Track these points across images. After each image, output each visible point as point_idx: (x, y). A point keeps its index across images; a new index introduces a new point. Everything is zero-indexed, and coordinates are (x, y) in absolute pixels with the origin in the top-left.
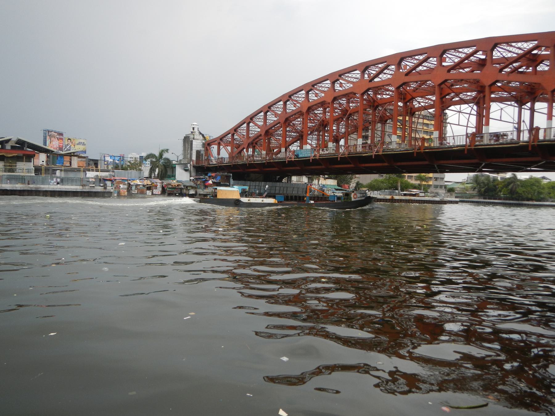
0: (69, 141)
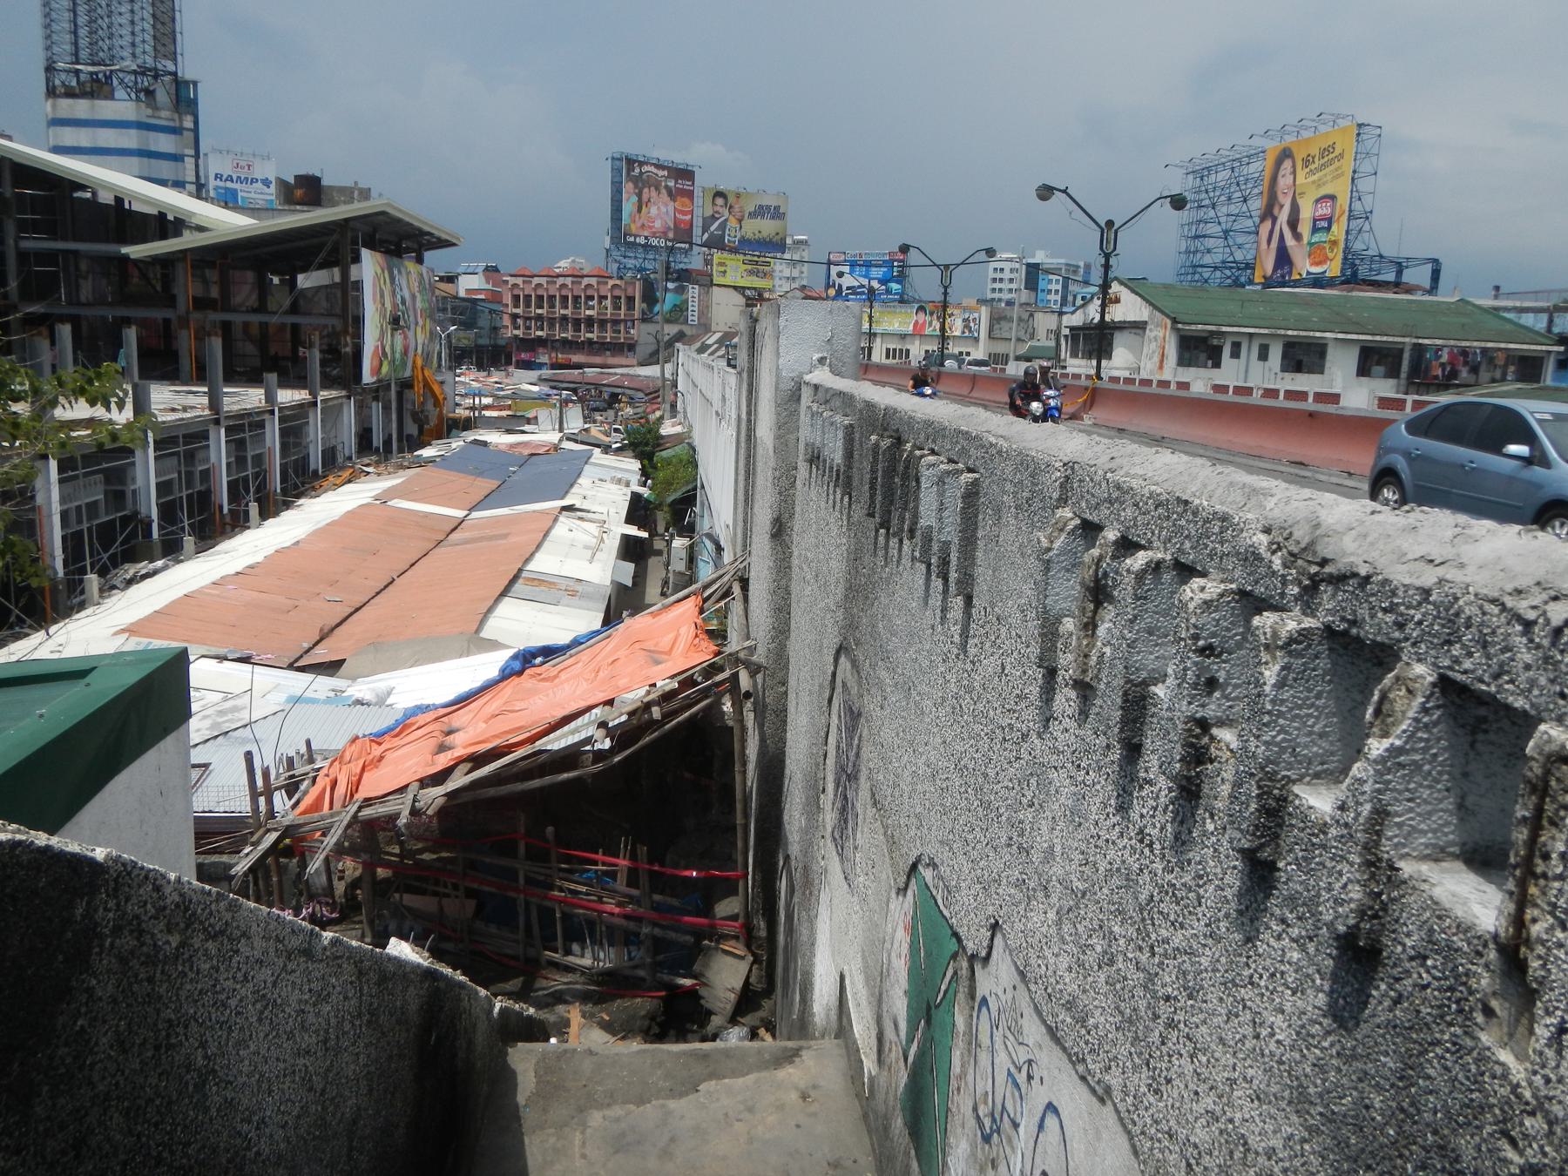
0: (720, 201)
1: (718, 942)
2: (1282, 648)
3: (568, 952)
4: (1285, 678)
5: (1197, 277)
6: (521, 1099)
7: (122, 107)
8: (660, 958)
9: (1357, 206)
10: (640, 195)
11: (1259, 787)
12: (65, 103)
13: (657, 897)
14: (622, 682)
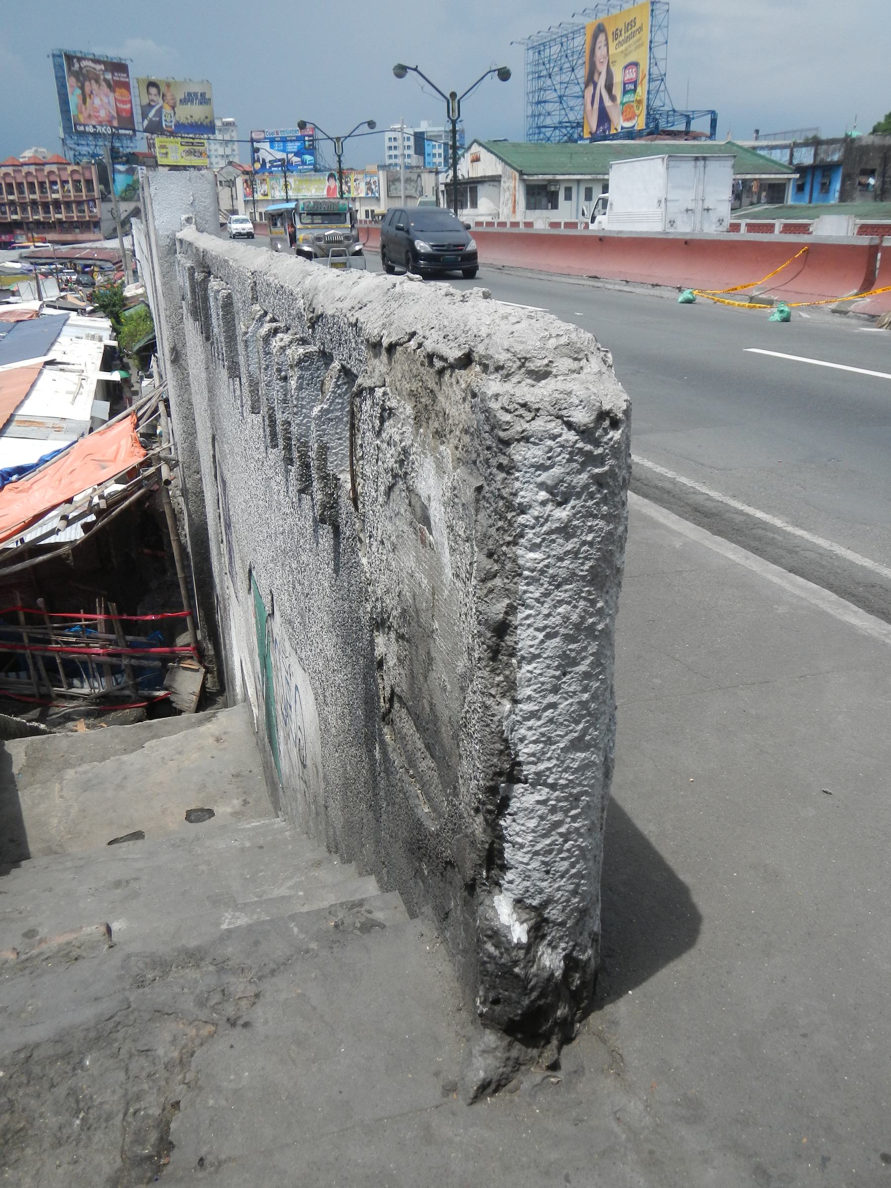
0: (153, 90)
1: (179, 662)
2: (296, 365)
3: (71, 686)
4: (301, 384)
5: (542, 136)
6: (15, 770)
8: (139, 680)
9: (655, 70)
10: (82, 88)
11: (299, 452)
13: (129, 638)
14: (77, 485)
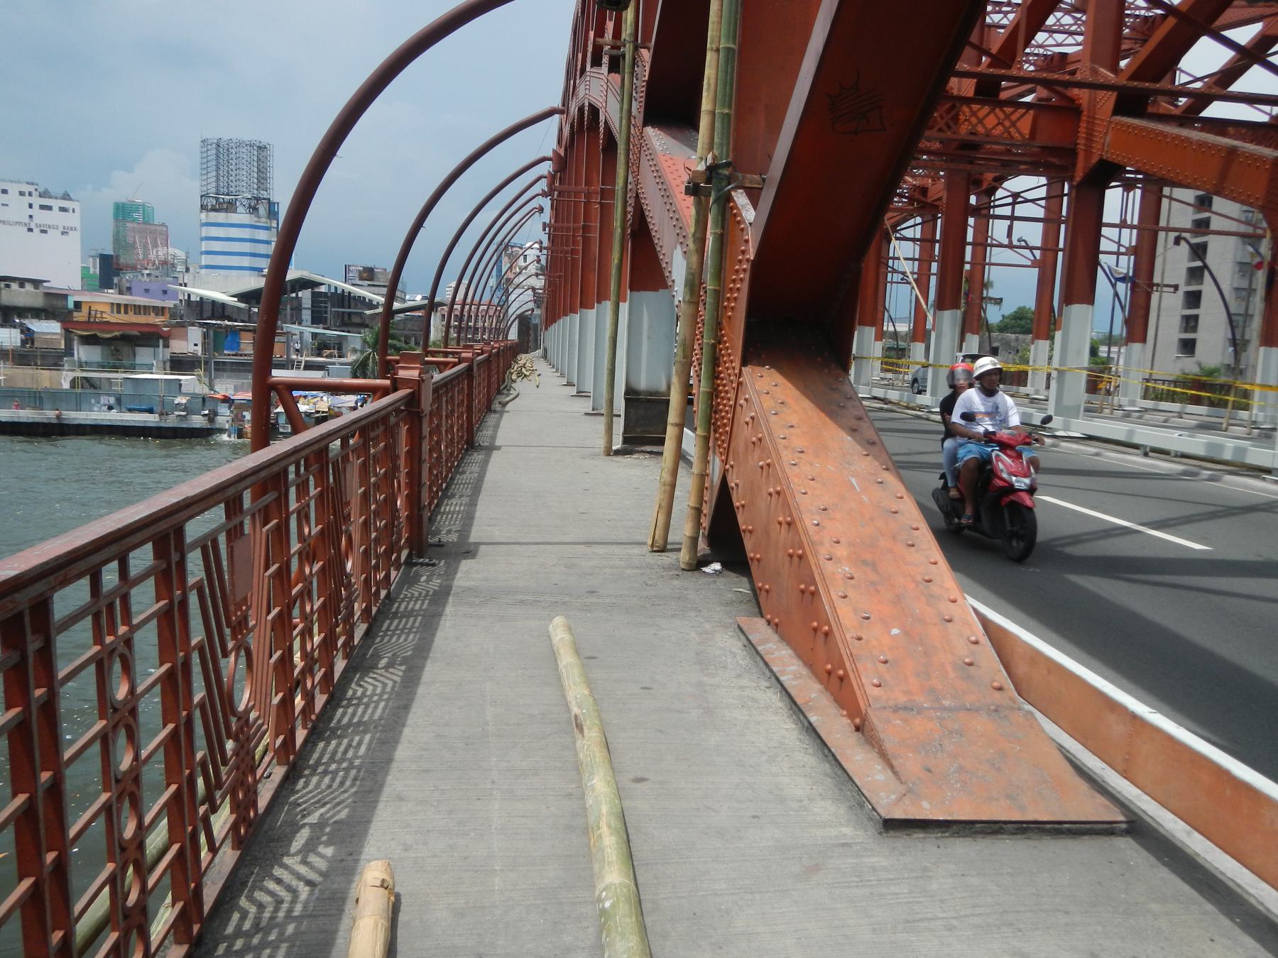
7: (242, 216)
12: (213, 214)
